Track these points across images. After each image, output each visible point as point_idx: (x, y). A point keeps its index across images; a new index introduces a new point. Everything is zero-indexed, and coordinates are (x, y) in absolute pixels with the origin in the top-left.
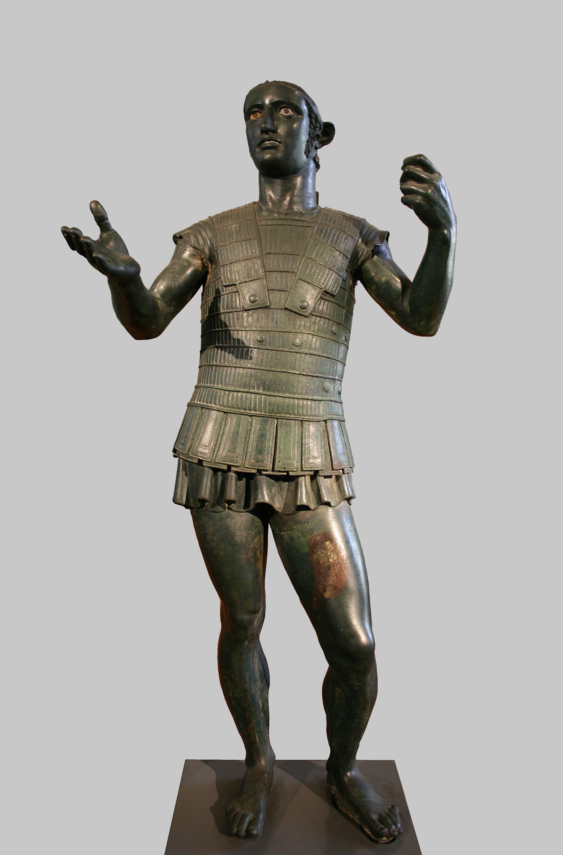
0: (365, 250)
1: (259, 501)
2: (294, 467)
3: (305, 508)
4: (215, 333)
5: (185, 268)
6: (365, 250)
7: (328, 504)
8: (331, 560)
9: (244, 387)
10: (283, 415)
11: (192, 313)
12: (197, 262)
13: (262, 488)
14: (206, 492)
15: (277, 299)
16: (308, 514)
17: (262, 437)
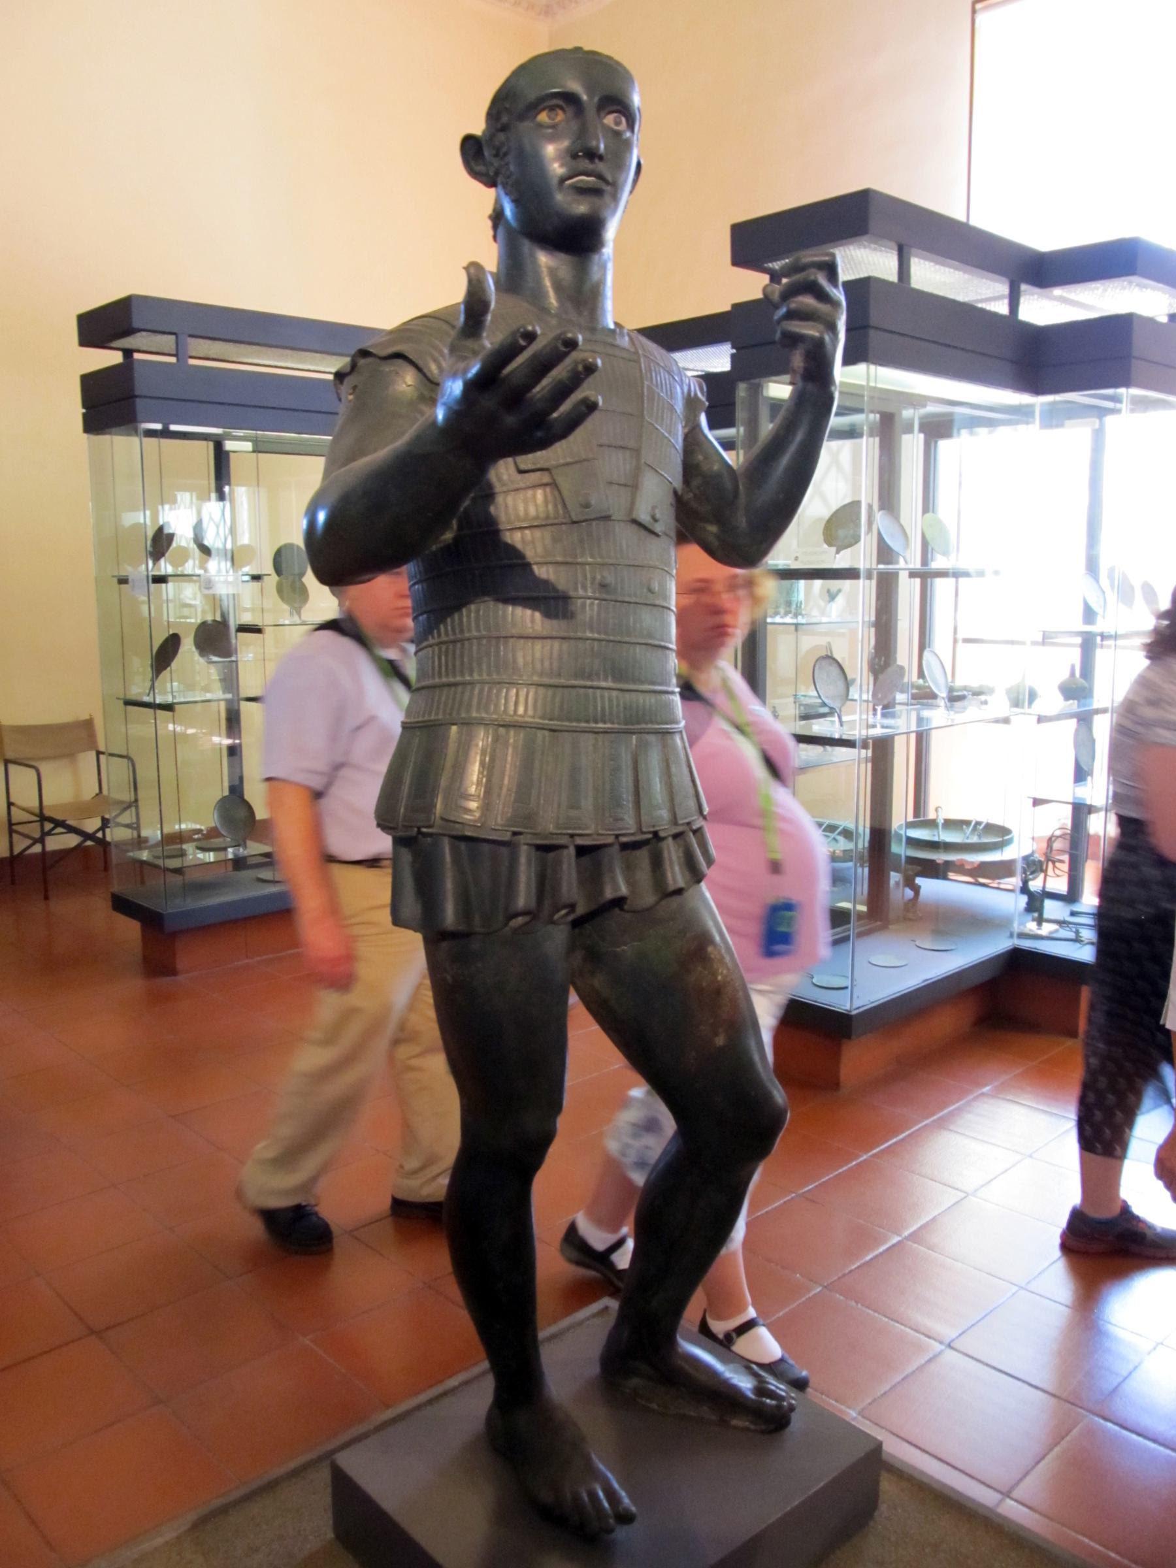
1: (609, 894)
3: (679, 892)
8: (720, 978)
9: (583, 677)
10: (643, 726)
13: (611, 870)
16: (675, 902)
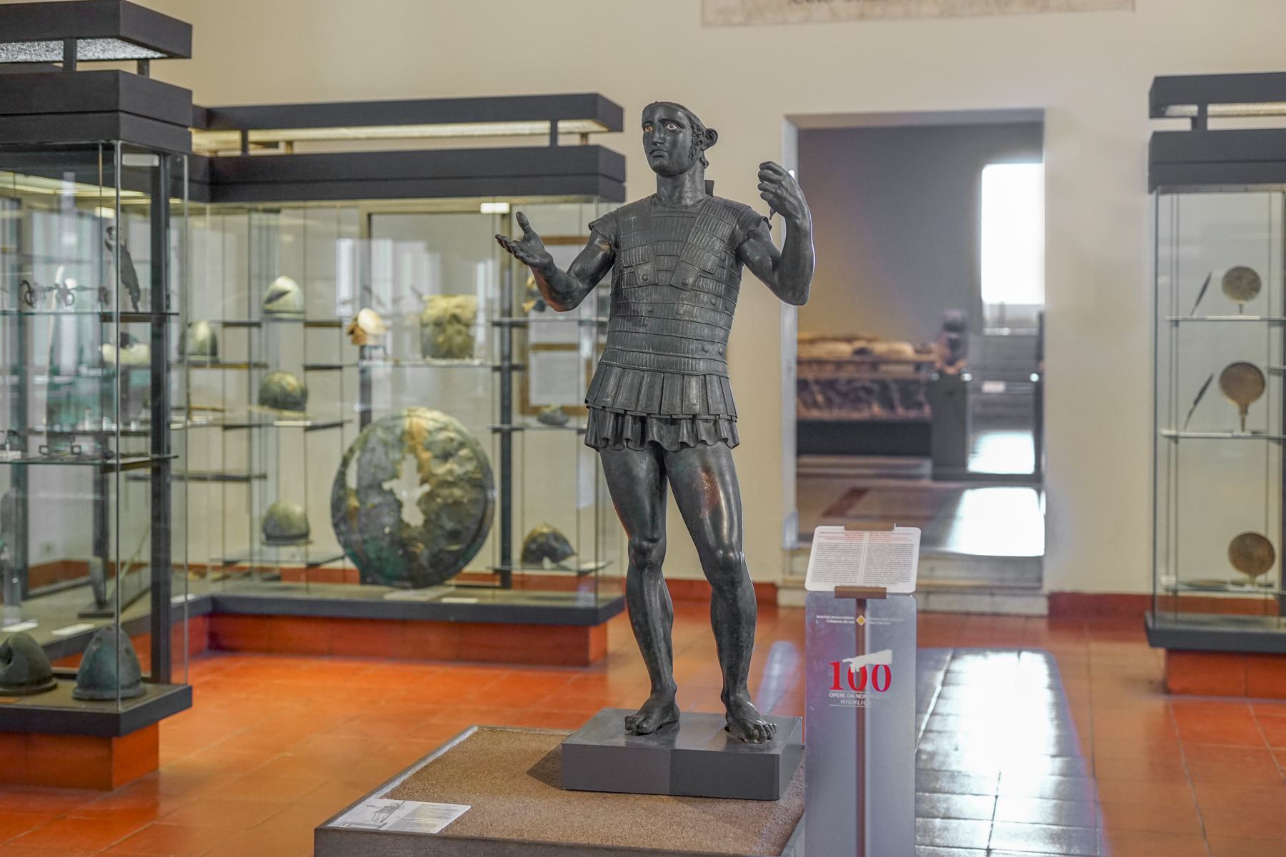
0: (741, 234)
2: (677, 412)
4: (619, 304)
5: (597, 253)
6: (741, 234)
7: (704, 442)
11: (604, 289)
12: (605, 247)
14: (609, 432)
15: (664, 277)
16: (690, 451)
17: (651, 387)
